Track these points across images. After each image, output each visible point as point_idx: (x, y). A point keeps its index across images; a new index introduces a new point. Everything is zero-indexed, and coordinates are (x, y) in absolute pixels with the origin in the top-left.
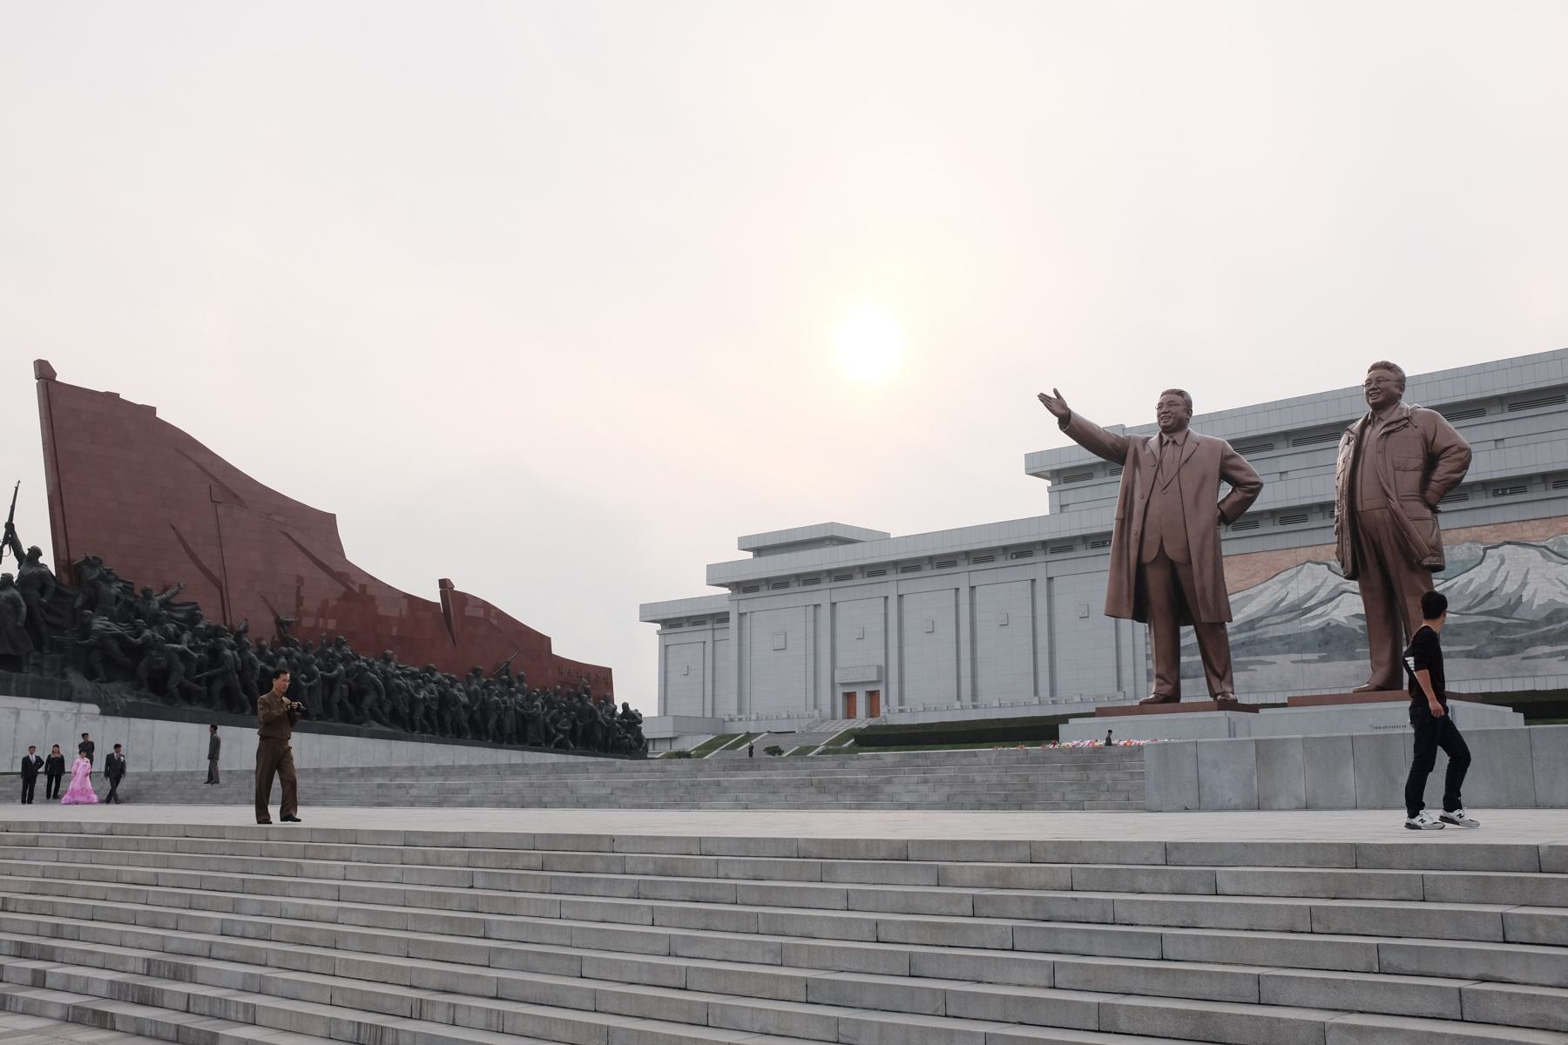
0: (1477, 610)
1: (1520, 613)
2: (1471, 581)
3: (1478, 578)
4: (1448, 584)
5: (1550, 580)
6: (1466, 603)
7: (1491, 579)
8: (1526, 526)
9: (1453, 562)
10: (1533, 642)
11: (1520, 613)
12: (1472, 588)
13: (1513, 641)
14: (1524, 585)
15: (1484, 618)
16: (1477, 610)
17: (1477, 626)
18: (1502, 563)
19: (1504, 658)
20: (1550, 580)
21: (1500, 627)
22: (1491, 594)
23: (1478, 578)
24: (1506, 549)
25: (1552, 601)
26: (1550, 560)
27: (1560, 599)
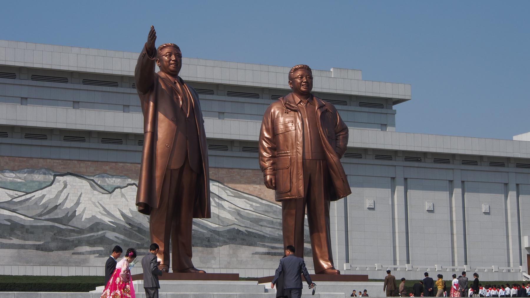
0: (47, 217)
1: (74, 223)
2: (44, 196)
3: (49, 194)
4: (28, 196)
5: (94, 203)
6: (39, 211)
7: (58, 196)
8: (82, 165)
9: (34, 182)
10: (80, 243)
11: (74, 223)
12: (44, 201)
13: (68, 241)
14: (78, 203)
15: (51, 223)
16: (47, 217)
17: (45, 228)
18: (65, 187)
19: (60, 253)
20: (94, 203)
21: (60, 231)
22: (56, 207)
23: (49, 194)
24: (69, 179)
25: (94, 217)
26: (95, 189)
27: (99, 216)
